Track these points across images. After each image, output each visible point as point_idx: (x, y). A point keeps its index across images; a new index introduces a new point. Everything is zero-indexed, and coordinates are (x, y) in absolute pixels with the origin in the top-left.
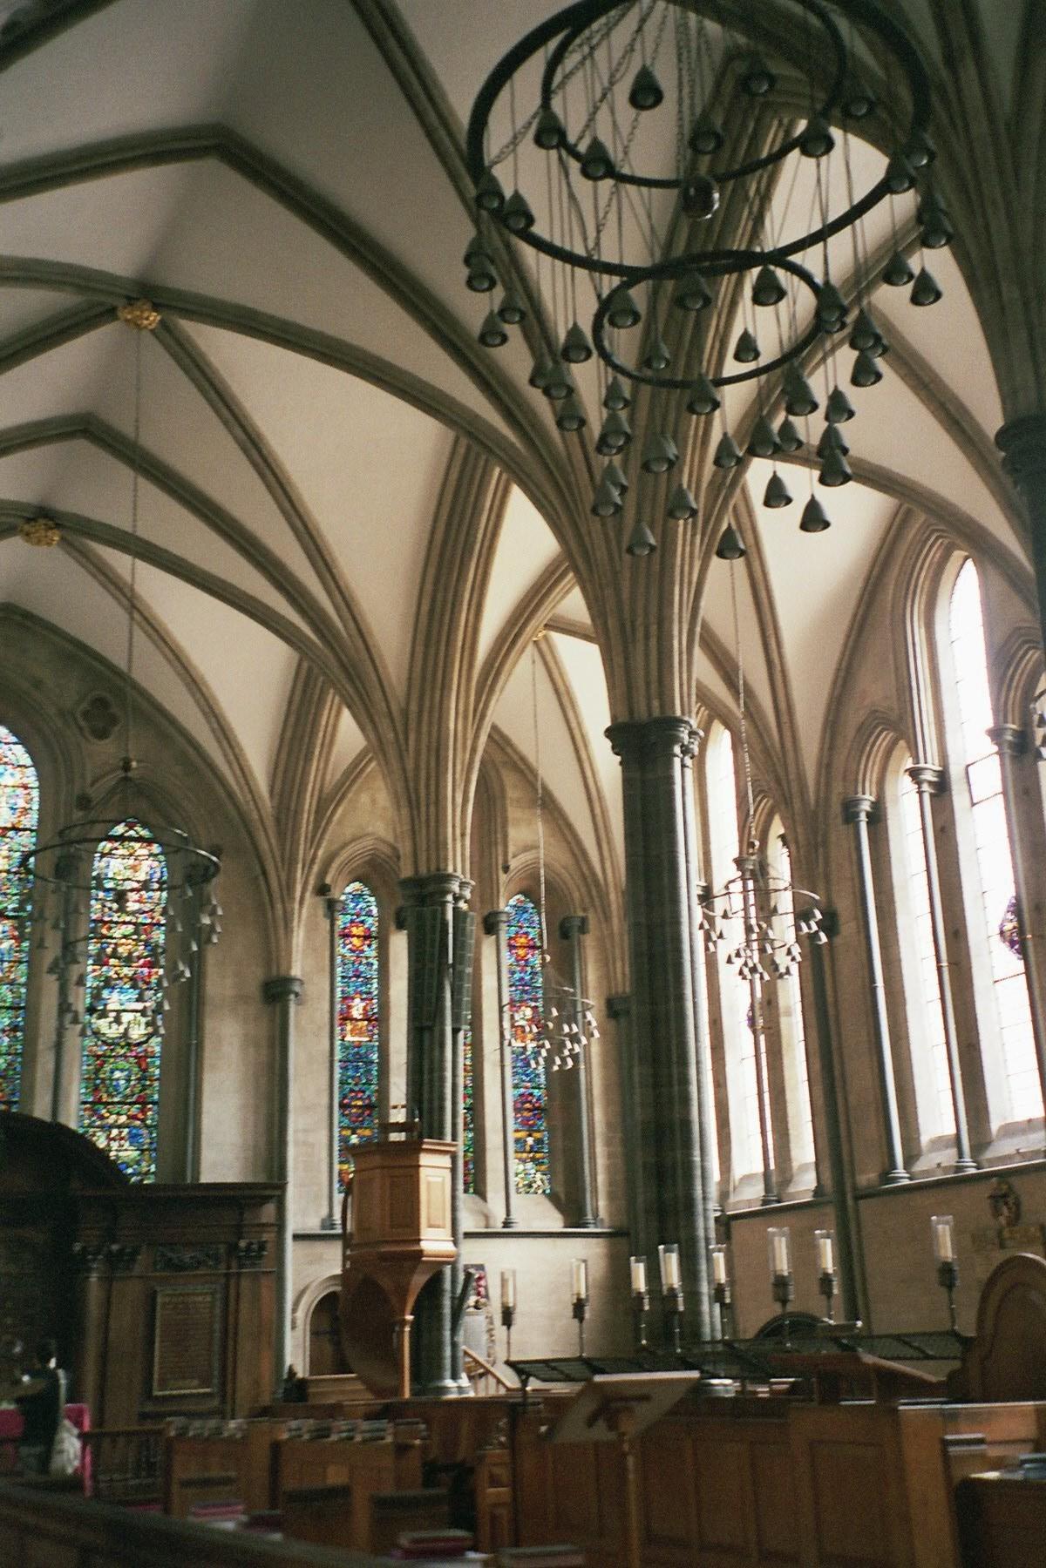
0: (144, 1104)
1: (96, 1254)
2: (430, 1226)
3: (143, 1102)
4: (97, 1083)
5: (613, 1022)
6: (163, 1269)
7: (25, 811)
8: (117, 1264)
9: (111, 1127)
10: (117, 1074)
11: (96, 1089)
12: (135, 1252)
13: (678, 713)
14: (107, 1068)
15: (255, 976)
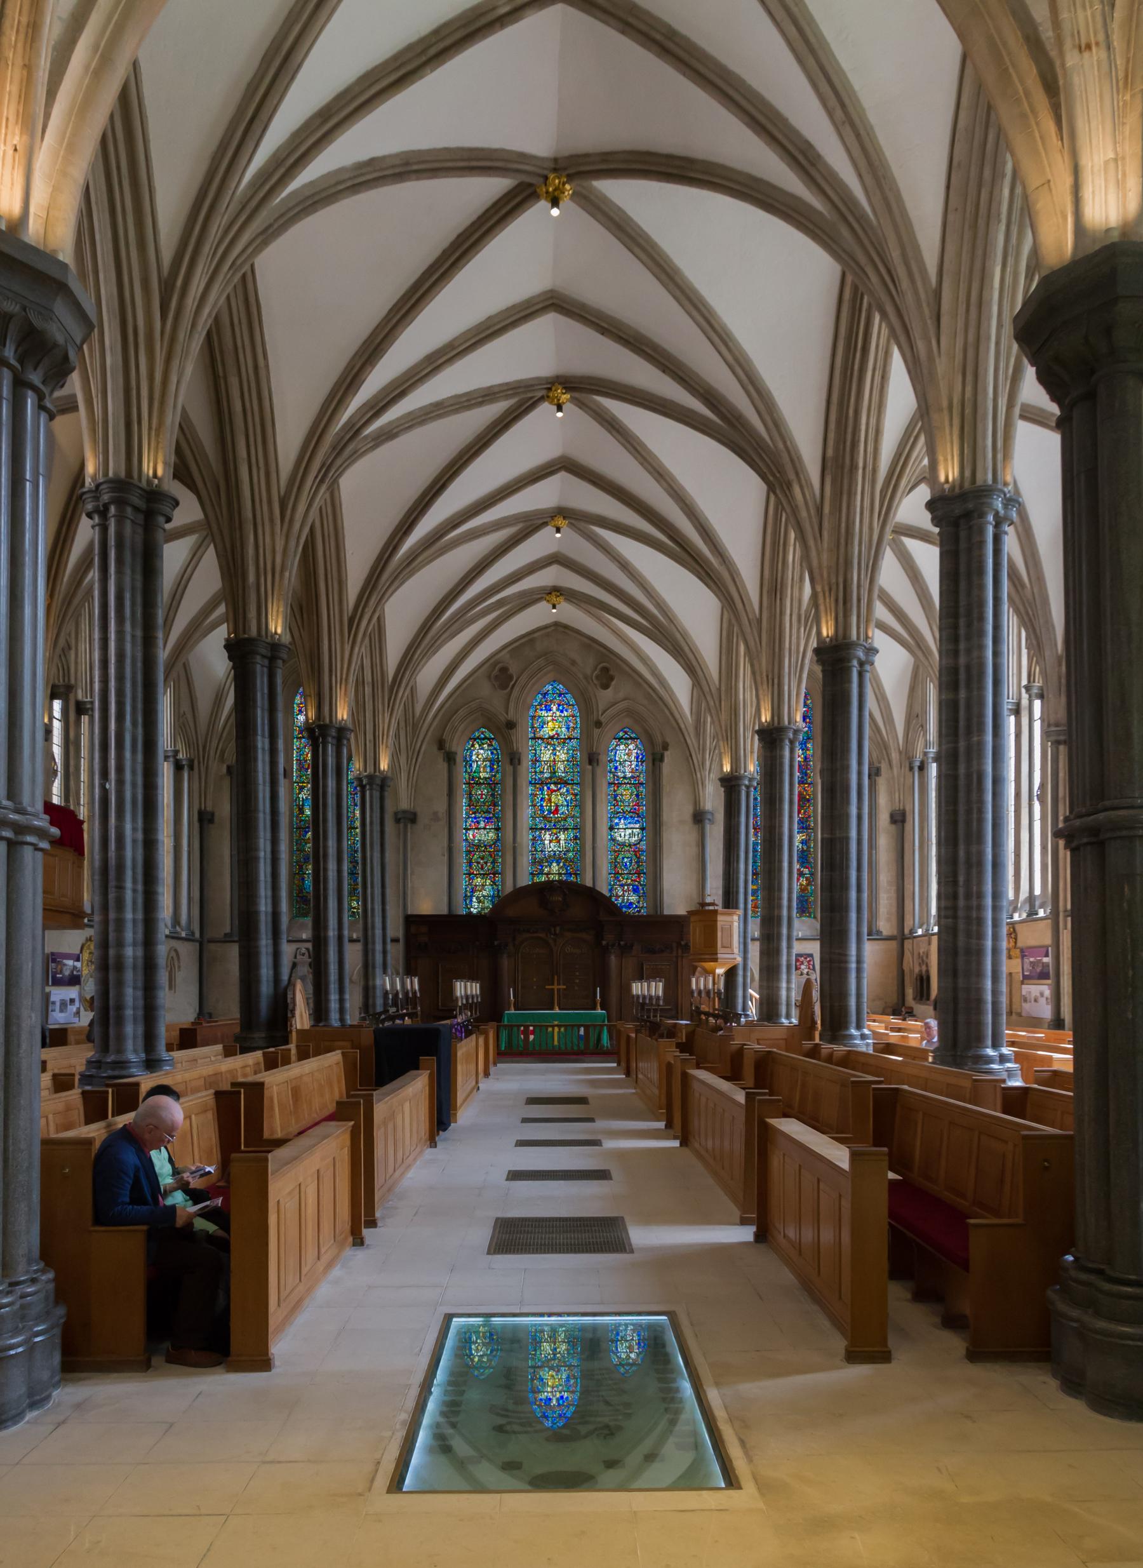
1: (613, 945)
2: (723, 947)
3: (638, 873)
4: (615, 864)
5: (894, 826)
7: (574, 728)
8: (625, 950)
12: (632, 946)
13: (786, 723)
14: (620, 857)
15: (688, 811)
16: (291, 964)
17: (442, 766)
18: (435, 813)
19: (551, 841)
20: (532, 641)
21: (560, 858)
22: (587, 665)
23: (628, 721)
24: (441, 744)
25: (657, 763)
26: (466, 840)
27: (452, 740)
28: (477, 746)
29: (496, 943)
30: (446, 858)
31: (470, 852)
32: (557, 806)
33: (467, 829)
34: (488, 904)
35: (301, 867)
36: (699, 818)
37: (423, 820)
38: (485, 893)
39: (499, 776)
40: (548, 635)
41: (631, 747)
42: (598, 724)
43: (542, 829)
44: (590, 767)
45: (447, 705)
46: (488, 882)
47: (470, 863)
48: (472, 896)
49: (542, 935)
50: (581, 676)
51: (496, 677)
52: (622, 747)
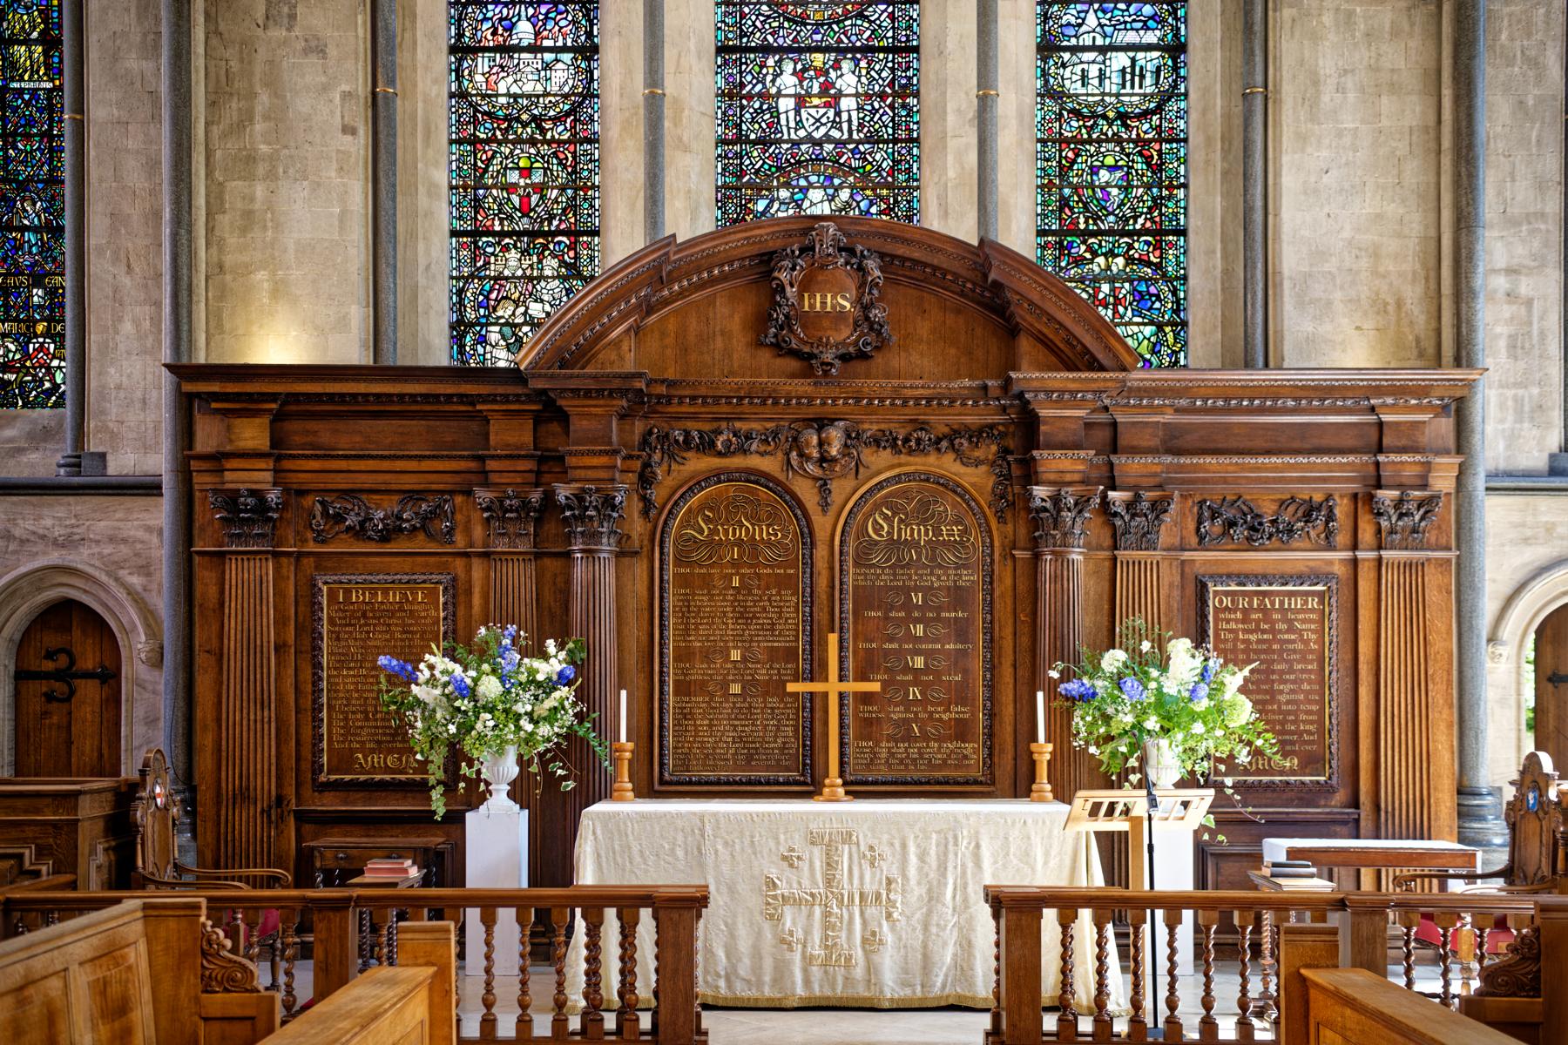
10: (1104, 175)
11: (1064, 203)
19: (801, 101)
26: (462, 95)
29: (563, 492)
31: (474, 141)
38: (536, 310)
43: (766, 49)
49: (769, 464)
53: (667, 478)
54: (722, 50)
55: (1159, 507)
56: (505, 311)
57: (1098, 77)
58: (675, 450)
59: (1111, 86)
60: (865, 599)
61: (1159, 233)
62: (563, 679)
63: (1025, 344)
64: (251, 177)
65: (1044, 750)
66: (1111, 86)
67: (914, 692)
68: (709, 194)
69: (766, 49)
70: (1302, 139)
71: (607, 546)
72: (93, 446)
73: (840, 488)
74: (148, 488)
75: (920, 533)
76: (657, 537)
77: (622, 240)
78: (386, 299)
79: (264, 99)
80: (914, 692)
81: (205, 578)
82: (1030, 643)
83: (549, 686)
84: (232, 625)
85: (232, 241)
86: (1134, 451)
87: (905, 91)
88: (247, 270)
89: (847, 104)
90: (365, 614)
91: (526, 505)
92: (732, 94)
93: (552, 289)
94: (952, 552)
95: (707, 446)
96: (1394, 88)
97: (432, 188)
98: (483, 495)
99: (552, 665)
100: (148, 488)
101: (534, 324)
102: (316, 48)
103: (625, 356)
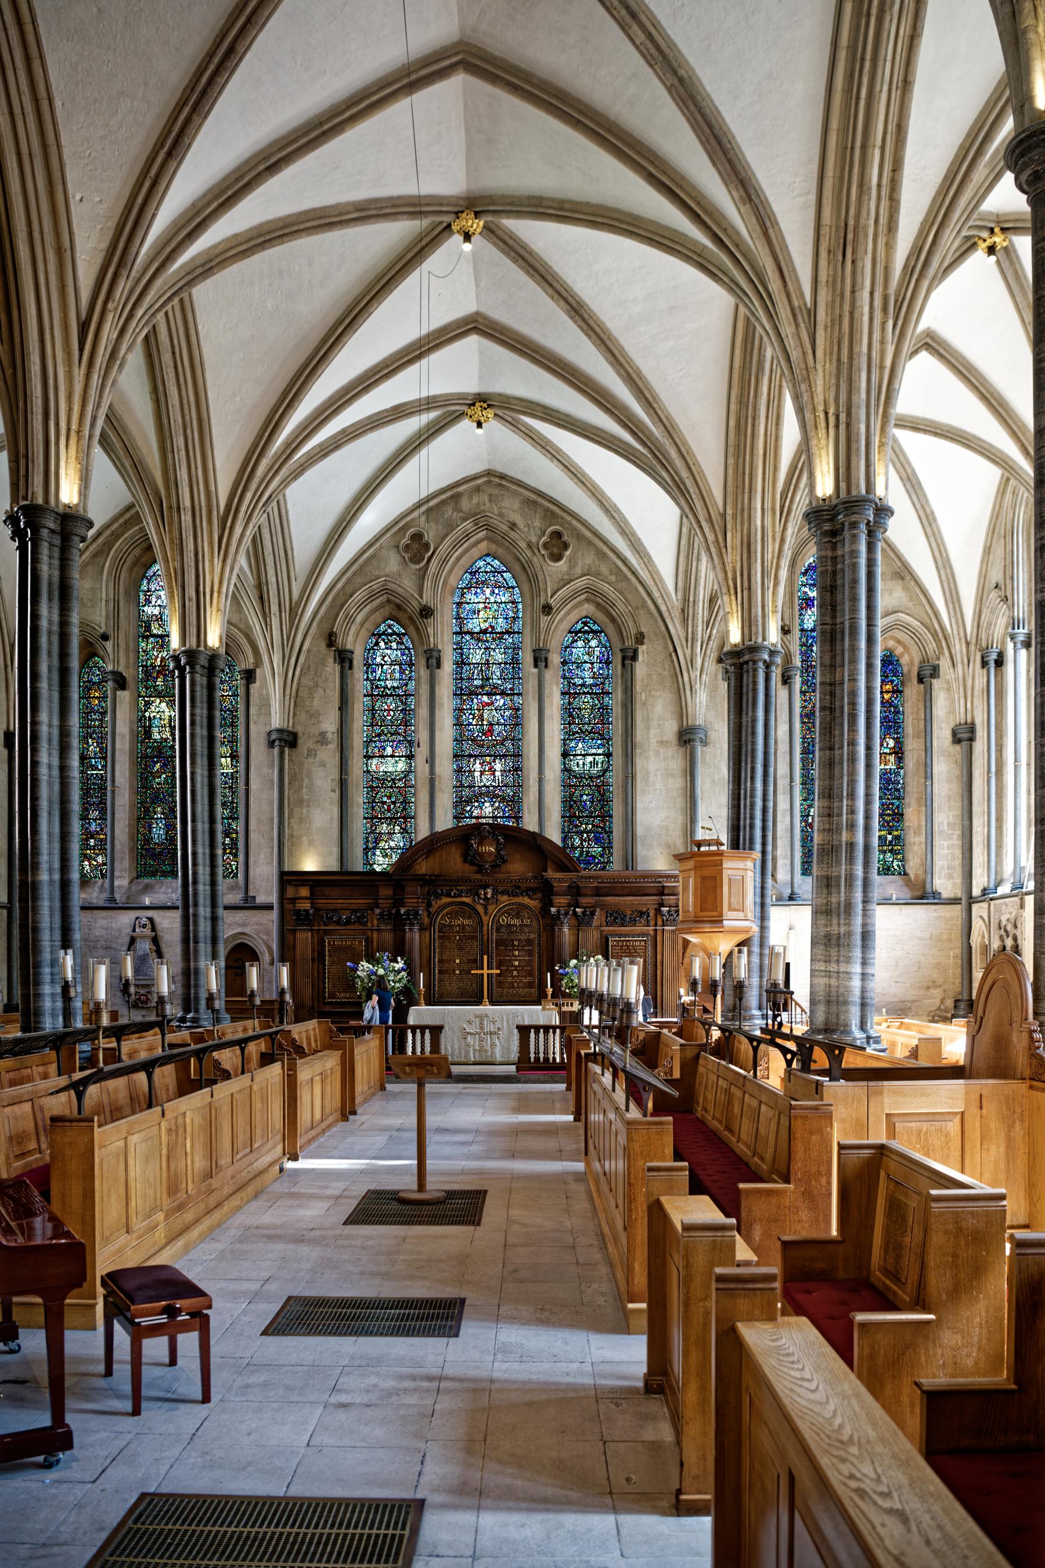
0: (603, 817)
6: (611, 925)
8: (581, 923)
9: (582, 833)
11: (571, 807)
15: (671, 728)
16: (127, 940)
17: (332, 669)
18: (323, 734)
19: (482, 773)
20: (456, 497)
21: (496, 796)
22: (531, 531)
23: (588, 609)
24: (331, 640)
25: (628, 662)
26: (368, 772)
27: (346, 634)
28: (382, 645)
30: (336, 796)
31: (372, 787)
32: (491, 725)
33: (368, 757)
34: (395, 858)
35: (147, 810)
36: (688, 737)
37: (305, 744)
38: (392, 844)
39: (412, 685)
40: (478, 489)
41: (593, 643)
42: (547, 609)
43: (470, 756)
44: (536, 671)
45: (339, 585)
46: (397, 828)
47: (372, 802)
48: (375, 848)
50: (523, 545)
51: (407, 547)
52: (580, 643)
53: (436, 904)
54: (455, 756)
55: (593, 914)
56: (382, 844)
57: (581, 764)
58: (438, 896)
59: (587, 767)
60: (500, 943)
61: (603, 817)
62: (403, 969)
63: (549, 863)
64: (301, 807)
65: (550, 990)
66: (587, 767)
67: (515, 973)
68: (451, 805)
69: (470, 756)
70: (643, 792)
71: (416, 928)
72: (251, 894)
73: (491, 908)
74: (269, 907)
75: (516, 922)
76: (432, 923)
77: (423, 832)
78: (345, 845)
79: (306, 782)
80: (515, 973)
81: (289, 937)
82: (552, 957)
83: (399, 972)
84: (298, 952)
85: (296, 827)
86: (586, 895)
87: (517, 769)
88: (300, 837)
89: (498, 774)
90: (339, 948)
91: (390, 914)
92: (459, 771)
93: (398, 837)
94: (527, 927)
95: (449, 895)
96: (673, 775)
97: (358, 806)
98: (377, 911)
99: (400, 965)
100: (269, 907)
101: (391, 848)
102: (323, 765)
103: (423, 867)
